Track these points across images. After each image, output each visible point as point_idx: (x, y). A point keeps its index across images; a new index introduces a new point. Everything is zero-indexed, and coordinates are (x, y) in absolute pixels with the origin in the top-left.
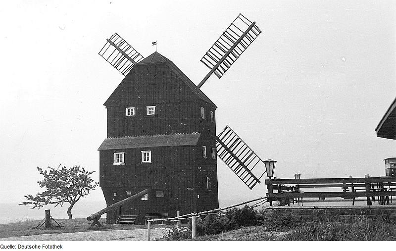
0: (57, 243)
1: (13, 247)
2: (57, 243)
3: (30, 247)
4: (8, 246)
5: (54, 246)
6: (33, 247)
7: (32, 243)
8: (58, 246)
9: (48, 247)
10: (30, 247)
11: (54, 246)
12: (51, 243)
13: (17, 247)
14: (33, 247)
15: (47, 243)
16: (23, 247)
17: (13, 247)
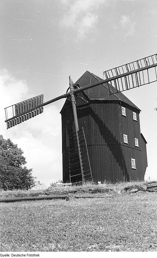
0: (36, 253)
1: (8, 255)
2: (36, 253)
3: (19, 256)
4: (5, 255)
5: (34, 255)
6: (21, 256)
7: (20, 253)
8: (37, 255)
9: (31, 255)
10: (19, 256)
11: (34, 255)
12: (32, 253)
13: (11, 255)
14: (21, 256)
15: (30, 253)
16: (14, 255)
17: (8, 255)
